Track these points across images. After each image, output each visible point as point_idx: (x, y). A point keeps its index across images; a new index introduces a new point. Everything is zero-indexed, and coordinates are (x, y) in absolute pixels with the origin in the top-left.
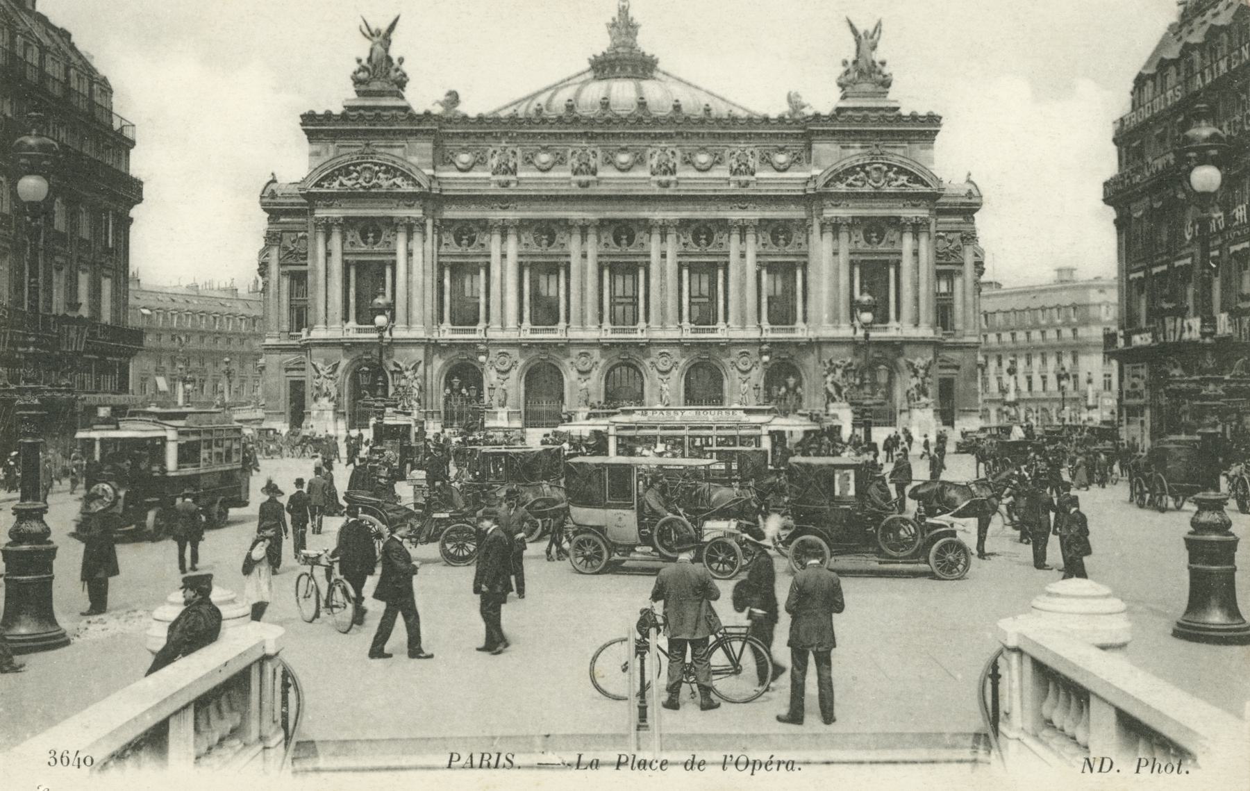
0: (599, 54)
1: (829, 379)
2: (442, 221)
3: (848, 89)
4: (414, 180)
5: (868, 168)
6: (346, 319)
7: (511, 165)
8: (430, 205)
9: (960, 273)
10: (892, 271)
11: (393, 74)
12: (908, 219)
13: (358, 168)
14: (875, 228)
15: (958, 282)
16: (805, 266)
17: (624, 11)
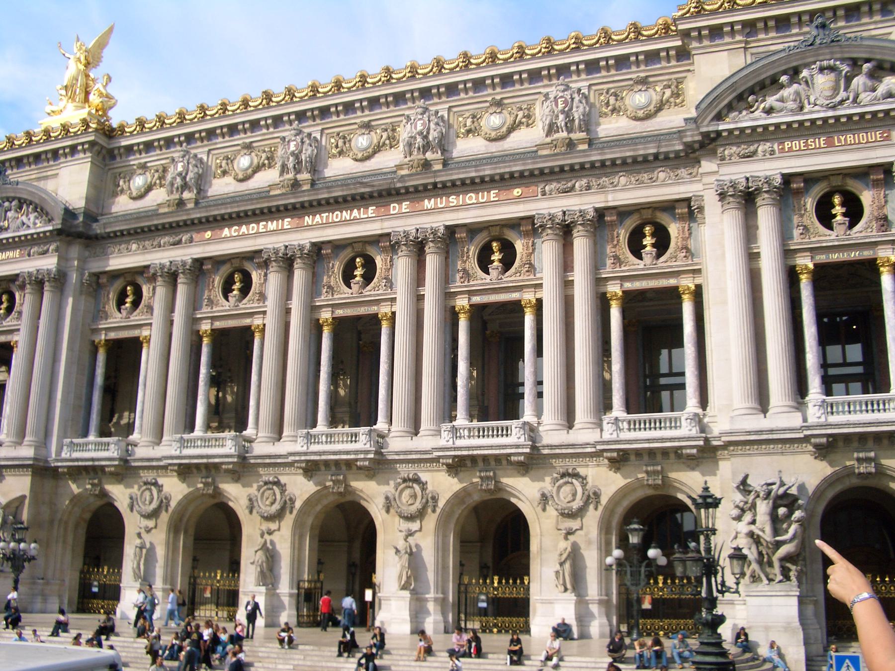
1: (743, 527)
2: (97, 275)
4: (47, 214)
5: (805, 73)
8: (75, 251)
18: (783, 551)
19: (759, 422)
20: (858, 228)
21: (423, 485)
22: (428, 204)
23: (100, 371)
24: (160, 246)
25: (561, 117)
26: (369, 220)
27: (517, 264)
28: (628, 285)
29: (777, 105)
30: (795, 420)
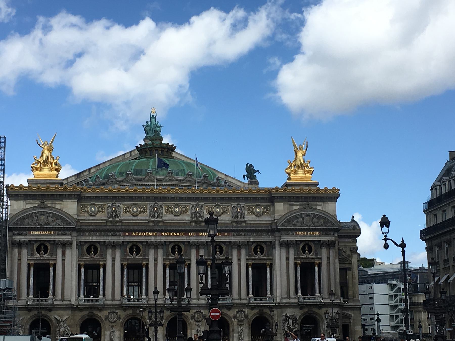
0: (143, 143)
1: (286, 325)
2: (80, 242)
3: (292, 175)
5: (303, 216)
6: (28, 294)
7: (118, 213)
8: (74, 234)
9: (350, 269)
10: (317, 268)
11: (53, 165)
12: (324, 242)
13: (38, 215)
14: (307, 246)
15: (349, 273)
16: (271, 266)
17: (153, 117)
18: (294, 330)
19: (287, 300)
20: (311, 254)
21: (202, 313)
22: (201, 234)
23: (83, 274)
24: (108, 235)
25: (239, 214)
26: (182, 236)
27: (224, 253)
28: (253, 262)
29: (296, 223)
30: (297, 301)
